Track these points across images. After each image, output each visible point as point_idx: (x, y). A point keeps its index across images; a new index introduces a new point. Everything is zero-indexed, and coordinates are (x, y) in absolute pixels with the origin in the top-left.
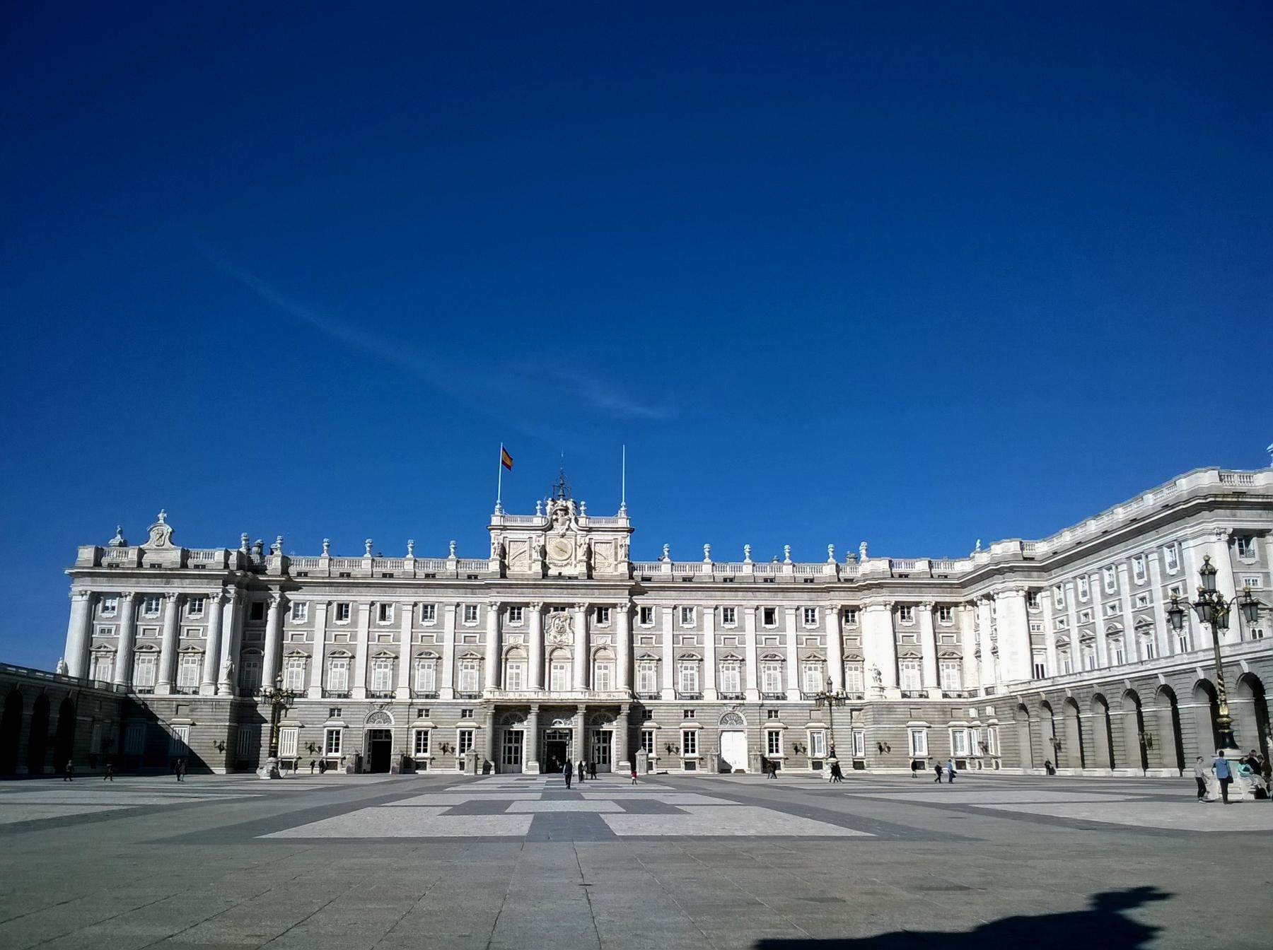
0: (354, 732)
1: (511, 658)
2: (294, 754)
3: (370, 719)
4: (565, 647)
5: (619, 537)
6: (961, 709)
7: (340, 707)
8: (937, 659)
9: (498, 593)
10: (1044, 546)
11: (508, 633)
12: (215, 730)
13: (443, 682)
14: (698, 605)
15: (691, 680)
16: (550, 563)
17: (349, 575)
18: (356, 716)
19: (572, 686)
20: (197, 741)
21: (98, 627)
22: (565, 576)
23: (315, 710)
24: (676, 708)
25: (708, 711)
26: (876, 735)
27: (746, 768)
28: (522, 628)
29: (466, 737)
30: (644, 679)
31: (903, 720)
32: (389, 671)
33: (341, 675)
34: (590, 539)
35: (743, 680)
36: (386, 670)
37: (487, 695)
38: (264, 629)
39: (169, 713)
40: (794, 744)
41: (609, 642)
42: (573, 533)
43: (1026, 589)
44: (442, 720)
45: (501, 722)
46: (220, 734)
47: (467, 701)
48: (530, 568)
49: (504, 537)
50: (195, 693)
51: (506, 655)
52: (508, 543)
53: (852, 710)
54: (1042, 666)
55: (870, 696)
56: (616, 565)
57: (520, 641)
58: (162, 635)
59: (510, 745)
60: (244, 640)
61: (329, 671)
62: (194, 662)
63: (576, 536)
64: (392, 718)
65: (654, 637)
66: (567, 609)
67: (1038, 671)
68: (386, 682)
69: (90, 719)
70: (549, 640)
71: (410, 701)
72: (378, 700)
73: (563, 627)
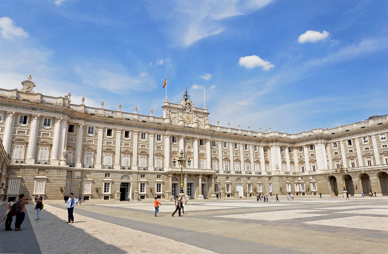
2: (90, 193)
3: (122, 178)
9: (170, 131)
12: (58, 182)
19: (193, 167)
20: (49, 187)
30: (214, 166)
31: (285, 181)
33: (109, 159)
37: (166, 170)
38: (75, 137)
39: (34, 173)
42: (191, 112)
44: (150, 179)
46: (61, 184)
47: (160, 171)
52: (171, 113)
53: (268, 177)
63: (192, 114)
65: (217, 151)
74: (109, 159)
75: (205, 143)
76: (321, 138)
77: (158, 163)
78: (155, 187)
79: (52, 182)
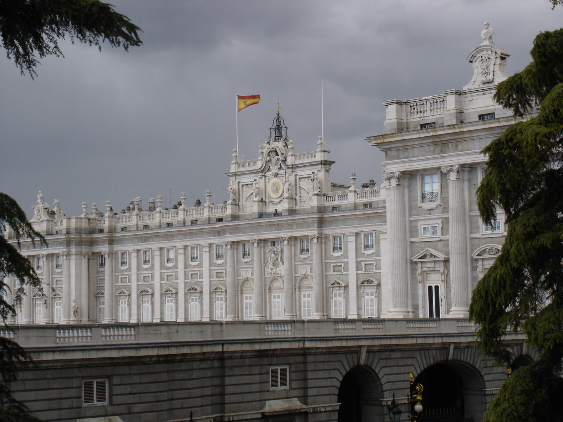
4: (279, 278)
9: (230, 233)
11: (242, 268)
15: (371, 306)
16: (269, 202)
28: (251, 263)
34: (296, 175)
41: (309, 272)
52: (241, 186)
73: (277, 260)
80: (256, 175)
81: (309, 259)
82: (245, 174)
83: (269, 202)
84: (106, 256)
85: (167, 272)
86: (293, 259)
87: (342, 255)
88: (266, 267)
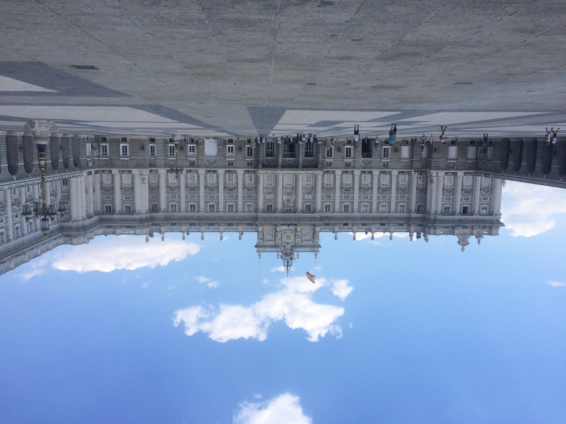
0: (377, 156)
1: (310, 188)
4: (286, 193)
5: (262, 243)
6: (103, 165)
7: (384, 167)
8: (113, 188)
9: (316, 217)
10: (60, 242)
11: (311, 200)
12: (438, 157)
13: (340, 178)
14: (226, 212)
16: (293, 231)
17: (382, 224)
18: (376, 163)
19: (283, 176)
21: (489, 201)
22: (287, 225)
23: (395, 166)
24: (237, 167)
25: (222, 165)
26: (145, 153)
27: (206, 140)
29: (330, 154)
30: (251, 180)
31: (132, 160)
32: (363, 182)
33: (383, 181)
34: (275, 242)
35: (206, 179)
36: (364, 183)
39: (457, 164)
40: (183, 150)
41: (267, 196)
42: (283, 245)
43: (70, 222)
44: (340, 162)
45: (314, 161)
46: (435, 156)
47: (329, 170)
48: (302, 229)
49: (314, 242)
50: (446, 173)
51: (313, 190)
52: (312, 240)
53: (156, 165)
54: (64, 185)
55: (146, 171)
56: (263, 230)
57: (306, 196)
58: (461, 198)
59: (310, 151)
60: (425, 196)
61: (389, 183)
62: (447, 186)
63: (281, 243)
64: (362, 163)
65: (246, 198)
66: (285, 211)
67: (66, 182)
68: (364, 178)
69: (493, 161)
70: (293, 198)
71: (354, 170)
72: (368, 170)
74: (383, 181)
75: (265, 208)
76: (78, 229)
77: (329, 179)
78: (335, 153)
79: (442, 157)
80: (301, 245)
81: (267, 202)
82: (308, 246)
83: (293, 231)
84: (413, 211)
85: (368, 200)
86: (276, 203)
87: (247, 203)
88: (295, 199)
